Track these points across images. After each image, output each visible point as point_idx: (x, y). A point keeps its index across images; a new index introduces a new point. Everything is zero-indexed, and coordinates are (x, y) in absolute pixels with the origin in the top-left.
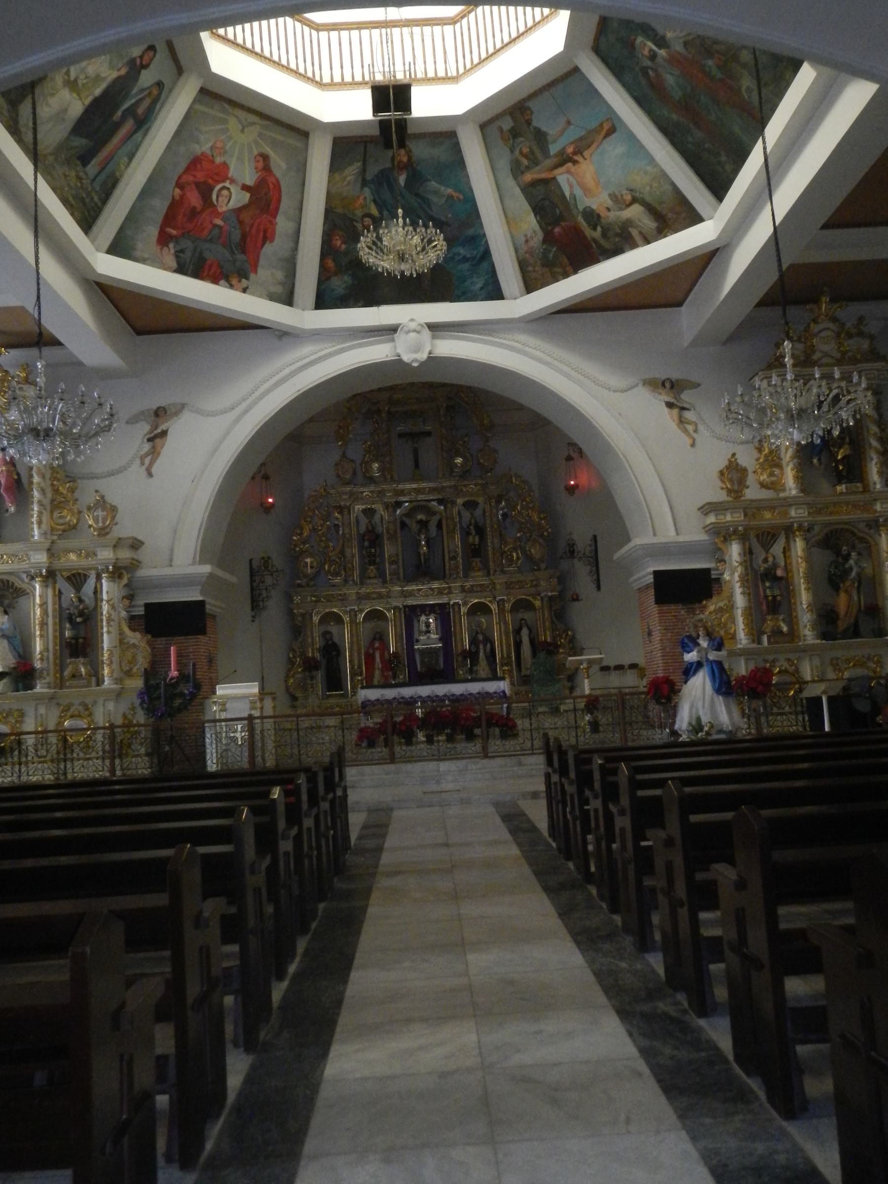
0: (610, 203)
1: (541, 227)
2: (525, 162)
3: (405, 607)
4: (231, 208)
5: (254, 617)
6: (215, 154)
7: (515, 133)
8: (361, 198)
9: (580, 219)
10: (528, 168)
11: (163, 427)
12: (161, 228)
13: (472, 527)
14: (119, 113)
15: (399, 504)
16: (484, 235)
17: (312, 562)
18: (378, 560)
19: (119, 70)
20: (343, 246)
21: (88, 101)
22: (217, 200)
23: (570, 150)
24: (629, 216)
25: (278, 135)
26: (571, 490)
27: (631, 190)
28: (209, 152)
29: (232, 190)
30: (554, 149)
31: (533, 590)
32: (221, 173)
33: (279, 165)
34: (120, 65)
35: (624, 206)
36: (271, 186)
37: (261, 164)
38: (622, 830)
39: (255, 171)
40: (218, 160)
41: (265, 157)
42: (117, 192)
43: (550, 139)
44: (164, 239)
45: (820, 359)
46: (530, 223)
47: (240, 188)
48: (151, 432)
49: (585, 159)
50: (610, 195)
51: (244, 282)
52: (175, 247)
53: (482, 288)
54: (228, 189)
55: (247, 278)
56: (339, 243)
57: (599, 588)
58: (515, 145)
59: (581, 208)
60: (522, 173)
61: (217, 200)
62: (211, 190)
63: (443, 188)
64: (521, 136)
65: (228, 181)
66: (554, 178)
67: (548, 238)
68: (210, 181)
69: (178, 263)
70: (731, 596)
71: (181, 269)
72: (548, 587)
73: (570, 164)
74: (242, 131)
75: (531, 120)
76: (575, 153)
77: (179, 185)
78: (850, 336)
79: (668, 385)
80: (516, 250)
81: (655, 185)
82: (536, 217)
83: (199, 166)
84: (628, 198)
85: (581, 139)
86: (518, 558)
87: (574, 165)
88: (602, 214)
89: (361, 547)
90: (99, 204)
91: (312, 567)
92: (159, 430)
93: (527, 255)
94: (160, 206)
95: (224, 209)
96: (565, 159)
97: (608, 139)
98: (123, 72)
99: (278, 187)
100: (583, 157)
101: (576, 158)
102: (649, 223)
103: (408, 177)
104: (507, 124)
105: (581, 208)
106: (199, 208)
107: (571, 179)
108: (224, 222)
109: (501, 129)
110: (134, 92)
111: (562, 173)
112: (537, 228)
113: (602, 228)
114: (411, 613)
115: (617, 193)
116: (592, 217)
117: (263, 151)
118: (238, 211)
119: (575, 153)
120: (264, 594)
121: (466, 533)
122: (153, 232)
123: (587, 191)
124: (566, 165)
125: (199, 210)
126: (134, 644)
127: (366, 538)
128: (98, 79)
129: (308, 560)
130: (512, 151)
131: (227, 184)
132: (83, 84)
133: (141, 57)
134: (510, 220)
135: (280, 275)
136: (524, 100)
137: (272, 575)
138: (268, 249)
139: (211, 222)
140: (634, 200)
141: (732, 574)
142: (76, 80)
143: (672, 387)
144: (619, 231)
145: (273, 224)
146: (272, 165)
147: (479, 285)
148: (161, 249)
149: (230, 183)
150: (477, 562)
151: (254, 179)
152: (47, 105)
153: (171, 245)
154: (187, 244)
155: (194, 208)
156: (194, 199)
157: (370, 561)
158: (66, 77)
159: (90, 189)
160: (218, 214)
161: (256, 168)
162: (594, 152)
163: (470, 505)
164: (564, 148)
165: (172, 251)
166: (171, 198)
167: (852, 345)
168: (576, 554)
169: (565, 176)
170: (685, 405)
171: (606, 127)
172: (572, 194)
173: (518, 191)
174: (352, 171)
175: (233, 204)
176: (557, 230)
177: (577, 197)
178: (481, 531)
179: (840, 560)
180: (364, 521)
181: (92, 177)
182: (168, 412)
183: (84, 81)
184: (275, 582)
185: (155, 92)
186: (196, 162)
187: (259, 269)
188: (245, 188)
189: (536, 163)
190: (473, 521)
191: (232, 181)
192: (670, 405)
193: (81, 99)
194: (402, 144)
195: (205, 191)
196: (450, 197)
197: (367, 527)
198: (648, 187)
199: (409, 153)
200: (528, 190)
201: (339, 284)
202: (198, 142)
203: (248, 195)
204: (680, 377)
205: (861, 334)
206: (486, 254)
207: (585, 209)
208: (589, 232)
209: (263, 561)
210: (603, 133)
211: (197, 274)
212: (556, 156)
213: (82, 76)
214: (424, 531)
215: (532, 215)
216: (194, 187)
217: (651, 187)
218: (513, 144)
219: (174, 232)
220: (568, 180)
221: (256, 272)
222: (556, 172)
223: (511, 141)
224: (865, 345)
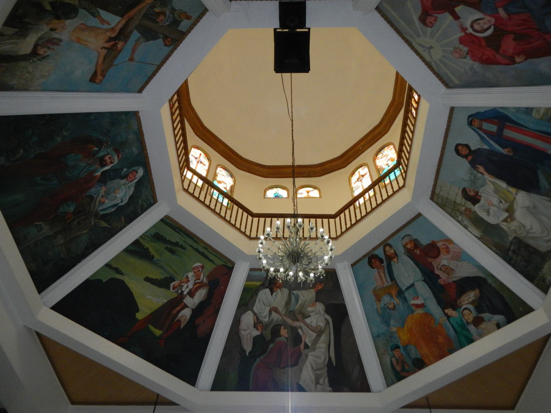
0: (56, 35)
6: (465, 53)
7: (176, 23)
14: (504, 151)
19: (482, 174)
21: (513, 190)
22: (489, 28)
24: (28, 39)
25: (402, 24)
27: (44, 58)
28: (468, 57)
29: (468, 25)
30: (136, 35)
34: (480, 175)
35: (40, 42)
37: (429, 19)
39: (438, 20)
40: (466, 49)
41: (423, 20)
47: (461, 20)
50: (61, 41)
54: (472, 26)
58: (172, 15)
64: (168, 25)
66: (122, 16)
68: (483, 43)
73: (113, 35)
74: (431, 48)
75: (164, 40)
77: (514, 62)
81: (28, 75)
83: (485, 57)
84: (41, 51)
85: (116, 57)
87: (110, 37)
88: (56, 21)
95: (488, 18)
98: (481, 169)
101: (112, 43)
104: (184, 25)
105: (82, 12)
106: (512, 36)
107: (106, 26)
108: (497, 9)
109: (188, 18)
110: (486, 147)
113: (47, 11)
115: (55, 47)
117: (422, 25)
119: (115, 45)
123: (85, 28)
125: (512, 36)
128: (497, 191)
130: (173, 10)
131: (470, 30)
132: (506, 202)
133: (465, 157)
136: (175, 49)
139: (510, 19)
140: (34, 53)
142: (507, 210)
144: (26, 20)
146: (420, 12)
149: (467, 29)
152: (531, 229)
155: (514, 39)
158: (509, 220)
160: (498, 19)
161: (436, 20)
162: (98, 57)
164: (126, 42)
166: (529, 60)
169: (113, 25)
171: (99, 77)
172: (98, 16)
175: (478, 15)
177: (91, 16)
183: (503, 202)
185: (476, 123)
186: (486, 61)
188: (456, 17)
189: (146, 16)
193: (515, 198)
198: (30, 70)
202: (472, 68)
203: (458, 9)
207: (77, 14)
212: (131, 32)
213: (502, 206)
216: (501, 51)
217: (29, 72)
218: (174, 14)
220: (109, 24)
222: (124, 21)
223: (176, 16)
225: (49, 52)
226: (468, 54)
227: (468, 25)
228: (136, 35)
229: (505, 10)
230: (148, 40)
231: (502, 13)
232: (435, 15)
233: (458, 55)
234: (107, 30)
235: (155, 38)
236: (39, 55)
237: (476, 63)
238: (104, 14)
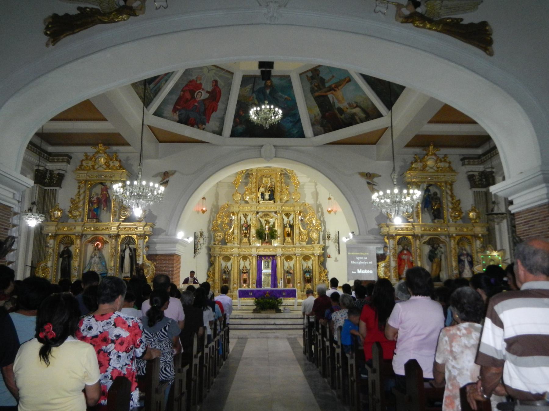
0: (348, 106)
1: (321, 113)
2: (316, 88)
3: (258, 256)
4: (203, 99)
5: (194, 256)
7: (312, 78)
8: (252, 97)
9: (336, 111)
10: (317, 91)
11: (167, 179)
12: (174, 106)
13: (288, 224)
15: (258, 213)
16: (299, 113)
17: (220, 235)
18: (248, 235)
20: (243, 114)
22: (196, 96)
23: (333, 86)
25: (222, 73)
26: (329, 212)
28: (195, 79)
29: (203, 92)
30: (327, 85)
31: (311, 252)
32: (199, 87)
33: (221, 83)
35: (353, 108)
36: (217, 91)
37: (214, 84)
38: (338, 354)
40: (198, 82)
41: (216, 81)
42: (159, 94)
43: (326, 81)
44: (175, 110)
45: (429, 170)
46: (317, 110)
48: (162, 181)
49: (339, 90)
51: (204, 126)
52: (179, 113)
53: (297, 133)
54: (201, 93)
55: (205, 125)
56: (241, 113)
57: (339, 253)
59: (337, 107)
60: (315, 92)
61: (196, 96)
62: (195, 92)
63: (284, 95)
65: (201, 90)
66: (327, 96)
67: (323, 117)
68: (195, 90)
69: (179, 118)
70: (389, 262)
71: (180, 121)
72: (318, 250)
73: (333, 91)
74: (209, 72)
75: (319, 74)
76: (336, 88)
77: (182, 90)
78: (441, 161)
79: (368, 175)
80: (311, 120)
82: (319, 108)
84: (355, 105)
85: (337, 82)
86: (306, 238)
89: (241, 230)
90: (153, 97)
91: (220, 237)
92: (165, 181)
93: (315, 122)
94: (175, 98)
95: (199, 99)
96: (331, 89)
97: (347, 84)
99: (220, 92)
100: (338, 89)
101: (335, 89)
102: (363, 115)
103: (270, 91)
104: (310, 74)
105: (337, 107)
107: (333, 96)
109: (307, 76)
111: (330, 94)
112: (319, 113)
114: (260, 257)
116: (341, 111)
118: (204, 100)
119: (335, 87)
120: (199, 247)
121: (285, 227)
122: (171, 107)
123: (339, 101)
124: (332, 91)
126: (149, 266)
127: (244, 226)
129: (219, 234)
130: (311, 84)
131: (201, 91)
134: (309, 108)
135: (218, 124)
137: (203, 239)
138: (214, 115)
140: (357, 106)
141: (390, 252)
143: (370, 176)
145: (217, 105)
146: (219, 84)
147: (296, 132)
148: (173, 114)
150: (288, 239)
151: (211, 89)
153: (177, 112)
154: (183, 111)
156: (188, 96)
157: (245, 236)
159: (150, 92)
160: (196, 101)
161: (212, 85)
163: (288, 215)
165: (178, 114)
167: (442, 165)
168: (330, 238)
170: (375, 184)
171: (347, 79)
172: (334, 103)
173: (313, 99)
174: (249, 87)
175: (202, 98)
176: (327, 114)
178: (291, 226)
179: (433, 250)
180: (243, 218)
181: (151, 89)
182: (169, 174)
184: (204, 242)
187: (210, 122)
188: (207, 92)
189: (320, 89)
190: (288, 222)
191: (203, 89)
192: (368, 183)
194: (269, 79)
195: (192, 92)
196: (286, 99)
197: (244, 222)
199: (272, 82)
200: (317, 99)
201: (240, 128)
204: (373, 172)
205: (445, 161)
206: (299, 120)
208: (339, 116)
209: (200, 233)
210: (345, 82)
211: (186, 124)
212: (328, 87)
214: (267, 224)
215: (318, 108)
219: (179, 107)
220: (332, 96)
221: (208, 122)
222: (328, 93)
224: (447, 165)
225: (353, 103)
226: (196, 81)
227: (203, 92)
228: (327, 85)
229: (196, 106)
230: (324, 80)
231: (196, 104)
232: (213, 87)
233: (199, 77)
234: (334, 95)
235: (321, 78)
236: (356, 105)
237: (192, 79)
238: (332, 101)
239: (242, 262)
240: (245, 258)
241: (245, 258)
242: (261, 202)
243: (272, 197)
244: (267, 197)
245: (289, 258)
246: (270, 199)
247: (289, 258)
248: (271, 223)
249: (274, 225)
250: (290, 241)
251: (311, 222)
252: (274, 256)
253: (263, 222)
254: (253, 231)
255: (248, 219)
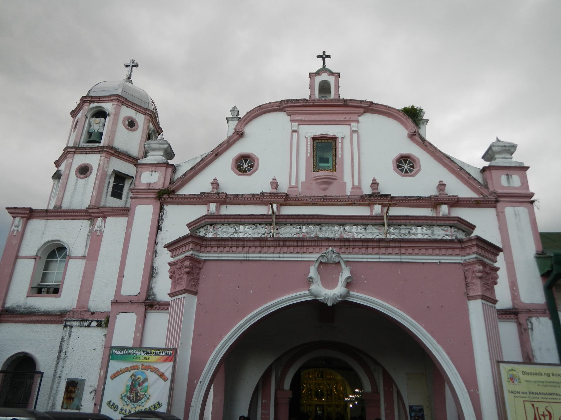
15: (315, 384)
114: (317, 406)
121: (328, 391)
150: (329, 397)
163: (329, 385)
239: (308, 408)
240: (310, 405)
241: (310, 405)
242: (317, 379)
243: (322, 377)
244: (320, 376)
245: (329, 406)
246: (321, 377)
247: (329, 406)
248: (322, 389)
249: (323, 390)
250: (330, 398)
251: (340, 389)
252: (323, 406)
253: (318, 387)
254: (314, 393)
255: (312, 386)
